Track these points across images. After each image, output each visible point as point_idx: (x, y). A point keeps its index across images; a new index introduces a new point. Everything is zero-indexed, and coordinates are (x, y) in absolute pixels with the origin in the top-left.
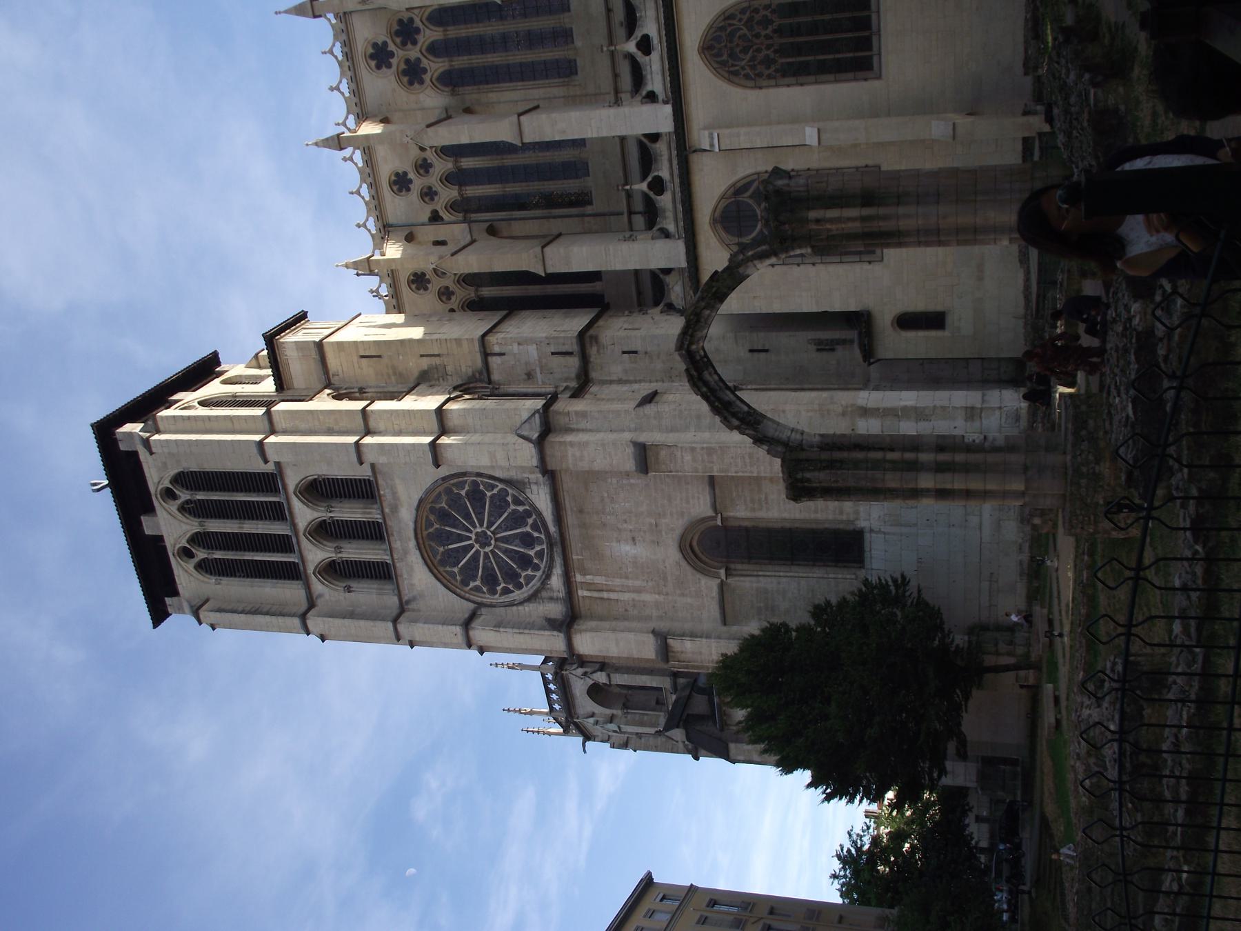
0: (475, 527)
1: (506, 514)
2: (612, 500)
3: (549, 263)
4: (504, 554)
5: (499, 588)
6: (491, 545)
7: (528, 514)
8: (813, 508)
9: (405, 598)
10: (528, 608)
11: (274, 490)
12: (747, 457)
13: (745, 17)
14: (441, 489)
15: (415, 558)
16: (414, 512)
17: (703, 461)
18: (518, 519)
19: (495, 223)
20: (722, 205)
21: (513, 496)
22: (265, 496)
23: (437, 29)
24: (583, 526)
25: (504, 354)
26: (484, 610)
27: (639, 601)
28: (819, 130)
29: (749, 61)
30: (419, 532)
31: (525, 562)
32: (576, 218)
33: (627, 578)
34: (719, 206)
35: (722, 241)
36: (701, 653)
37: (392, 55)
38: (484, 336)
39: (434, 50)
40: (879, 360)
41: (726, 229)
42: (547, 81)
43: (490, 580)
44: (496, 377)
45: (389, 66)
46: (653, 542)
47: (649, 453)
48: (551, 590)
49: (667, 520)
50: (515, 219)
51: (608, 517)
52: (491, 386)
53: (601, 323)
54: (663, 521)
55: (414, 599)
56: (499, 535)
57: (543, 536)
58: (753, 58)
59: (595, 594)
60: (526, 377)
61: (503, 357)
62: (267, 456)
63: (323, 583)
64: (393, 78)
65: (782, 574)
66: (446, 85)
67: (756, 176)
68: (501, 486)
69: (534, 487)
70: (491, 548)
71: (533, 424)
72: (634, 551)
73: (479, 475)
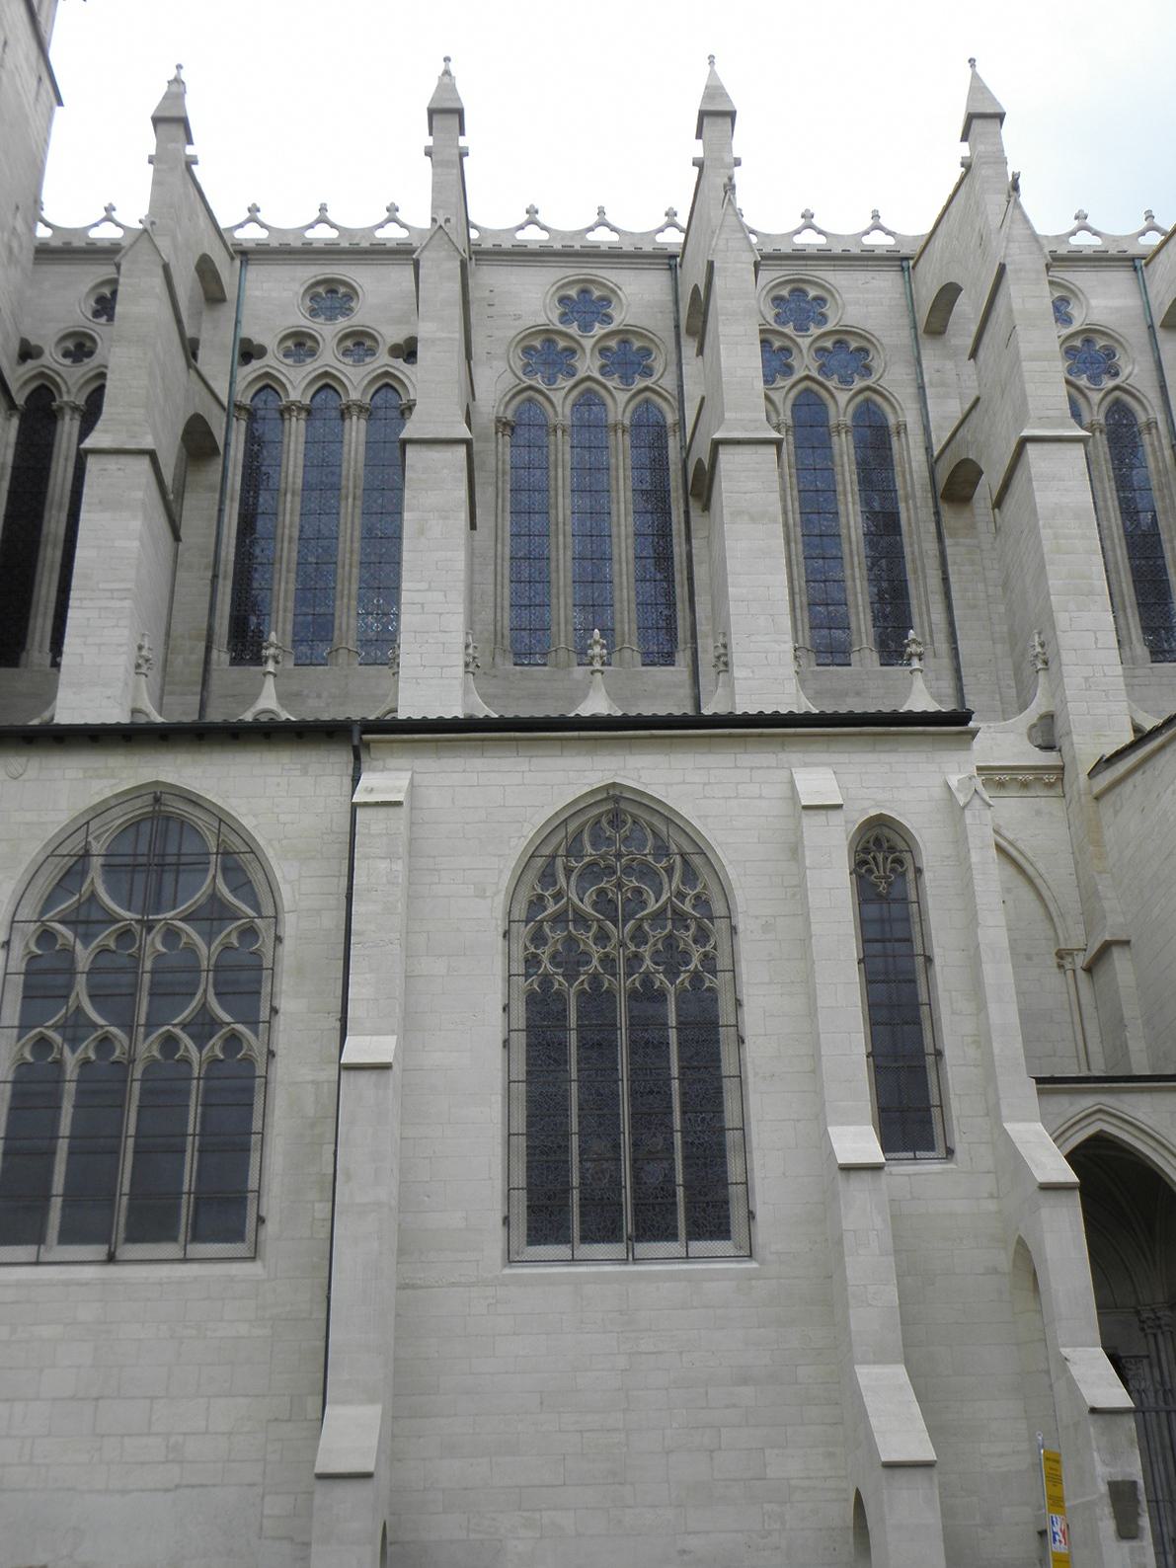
3: (112, 464)
13: (687, 907)
19: (220, 460)
23: (628, 414)
28: (385, 1067)
29: (577, 911)
32: (205, 626)
34: (198, 812)
35: (100, 810)
37: (586, 327)
39: (589, 399)
42: (507, 604)
45: (564, 318)
50: (222, 502)
58: (581, 920)
64: (542, 320)
66: (518, 412)
67: (268, 911)
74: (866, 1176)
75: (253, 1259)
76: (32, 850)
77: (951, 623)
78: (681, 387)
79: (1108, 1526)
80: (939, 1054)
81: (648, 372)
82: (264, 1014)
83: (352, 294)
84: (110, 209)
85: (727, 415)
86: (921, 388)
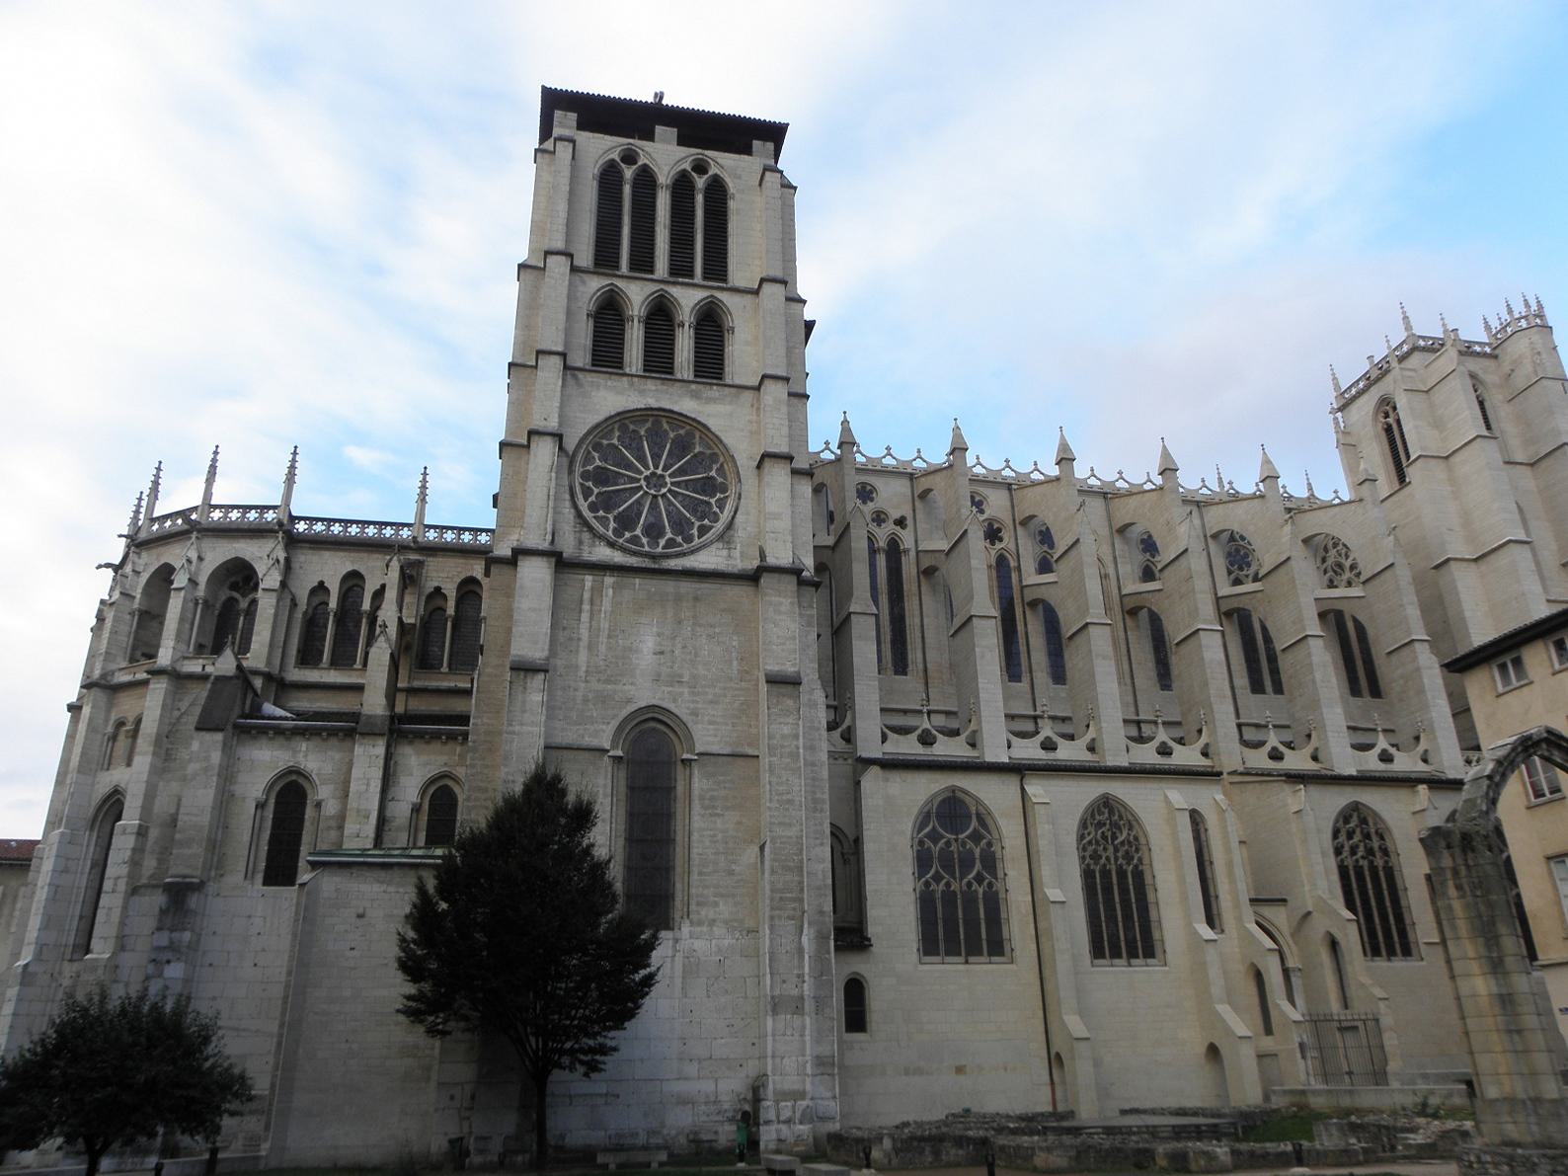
3: (862, 619)
4: (636, 501)
5: (590, 484)
7: (689, 539)
9: (580, 375)
11: (708, 274)
12: (789, 797)
13: (1131, 838)
16: (693, 416)
17: (782, 746)
18: (680, 526)
20: (967, 799)
24: (678, 599)
27: (578, 646)
30: (667, 414)
31: (626, 522)
33: (609, 637)
36: (524, 711)
41: (943, 801)
43: (601, 477)
47: (790, 688)
48: (593, 545)
49: (686, 695)
51: (689, 629)
54: (686, 690)
55: (579, 384)
56: (659, 498)
57: (659, 550)
59: (587, 596)
63: (598, 291)
65: (613, 826)
68: (725, 517)
69: (725, 552)
72: (645, 651)
74: (1212, 943)
75: (1012, 963)
76: (915, 811)
77: (1131, 671)
78: (1018, 551)
79: (1299, 1055)
80: (1217, 897)
81: (1001, 540)
82: (1000, 874)
83: (874, 489)
85: (1091, 611)
86: (1115, 558)
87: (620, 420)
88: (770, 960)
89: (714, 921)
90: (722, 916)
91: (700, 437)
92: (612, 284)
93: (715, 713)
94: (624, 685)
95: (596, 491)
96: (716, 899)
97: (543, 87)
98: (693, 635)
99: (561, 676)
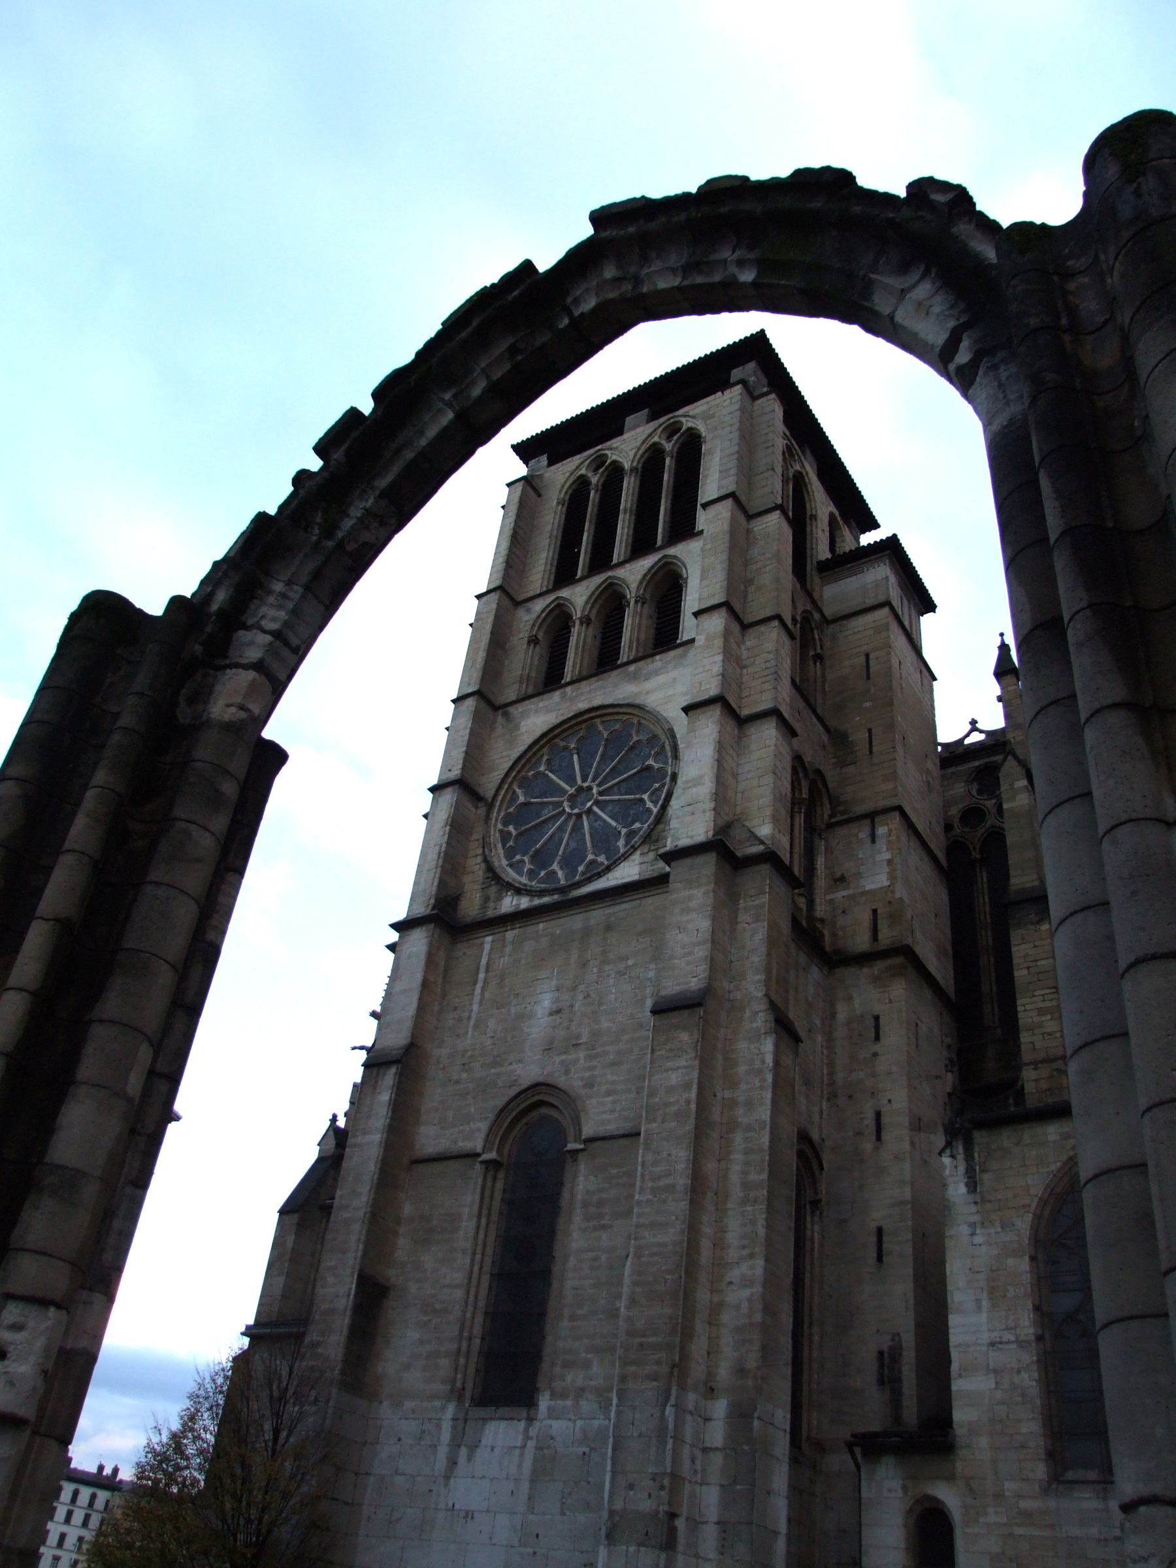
0: (599, 785)
1: (614, 824)
2: (620, 974)
5: (511, 828)
6: (572, 809)
8: (580, 1312)
9: (511, 709)
10: (475, 866)
14: (658, 731)
15: (567, 711)
17: (667, 1105)
18: (604, 840)
21: (640, 829)
22: (664, 529)
24: (587, 933)
25: (873, 841)
26: (482, 811)
31: (541, 859)
38: (899, 809)
40: (858, 1467)
44: (841, 832)
46: (551, 1042)
48: (499, 899)
49: (582, 1061)
51: (595, 970)
52: (823, 826)
53: (928, 994)
56: (585, 818)
59: (484, 961)
60: (838, 875)
61: (869, 840)
62: (712, 506)
68: (655, 810)
70: (568, 810)
71: (749, 844)
73: (674, 777)
84: (973, 722)
87: (548, 742)
88: (614, 1450)
89: (583, 1390)
90: (593, 1383)
91: (603, 722)
92: (558, 598)
93: (615, 1078)
94: (511, 1064)
95: (514, 833)
96: (589, 1356)
97: (513, 447)
98: (598, 977)
99: (444, 1069)
